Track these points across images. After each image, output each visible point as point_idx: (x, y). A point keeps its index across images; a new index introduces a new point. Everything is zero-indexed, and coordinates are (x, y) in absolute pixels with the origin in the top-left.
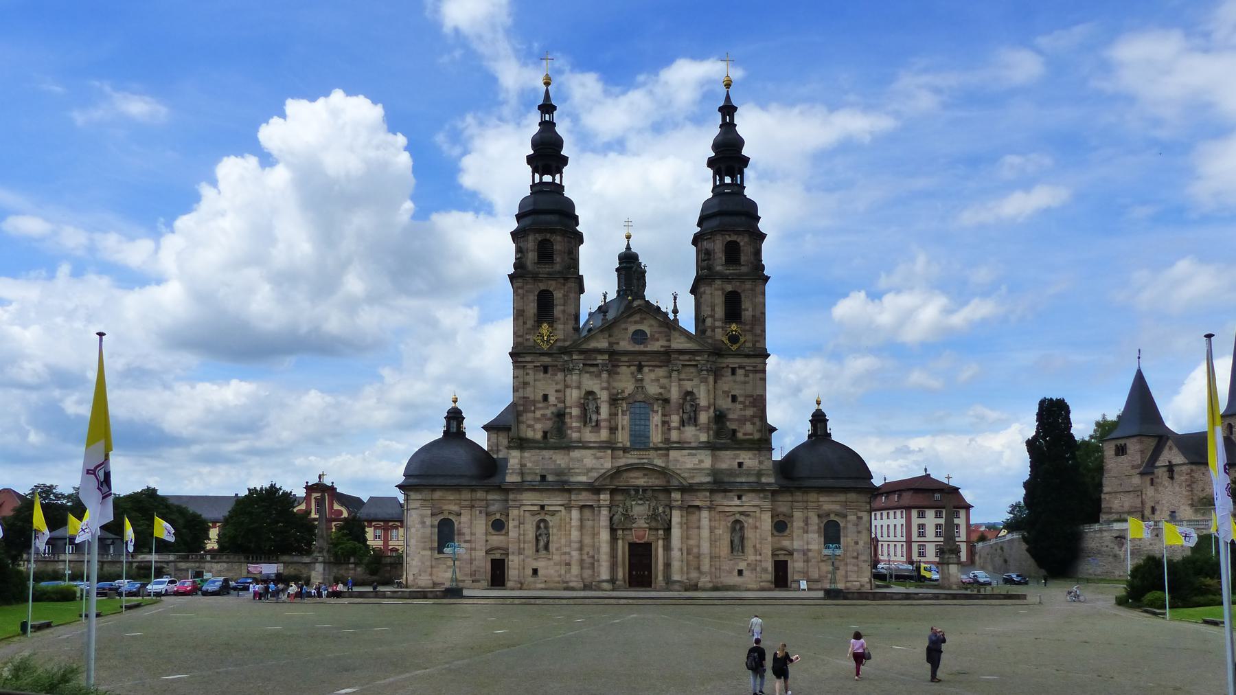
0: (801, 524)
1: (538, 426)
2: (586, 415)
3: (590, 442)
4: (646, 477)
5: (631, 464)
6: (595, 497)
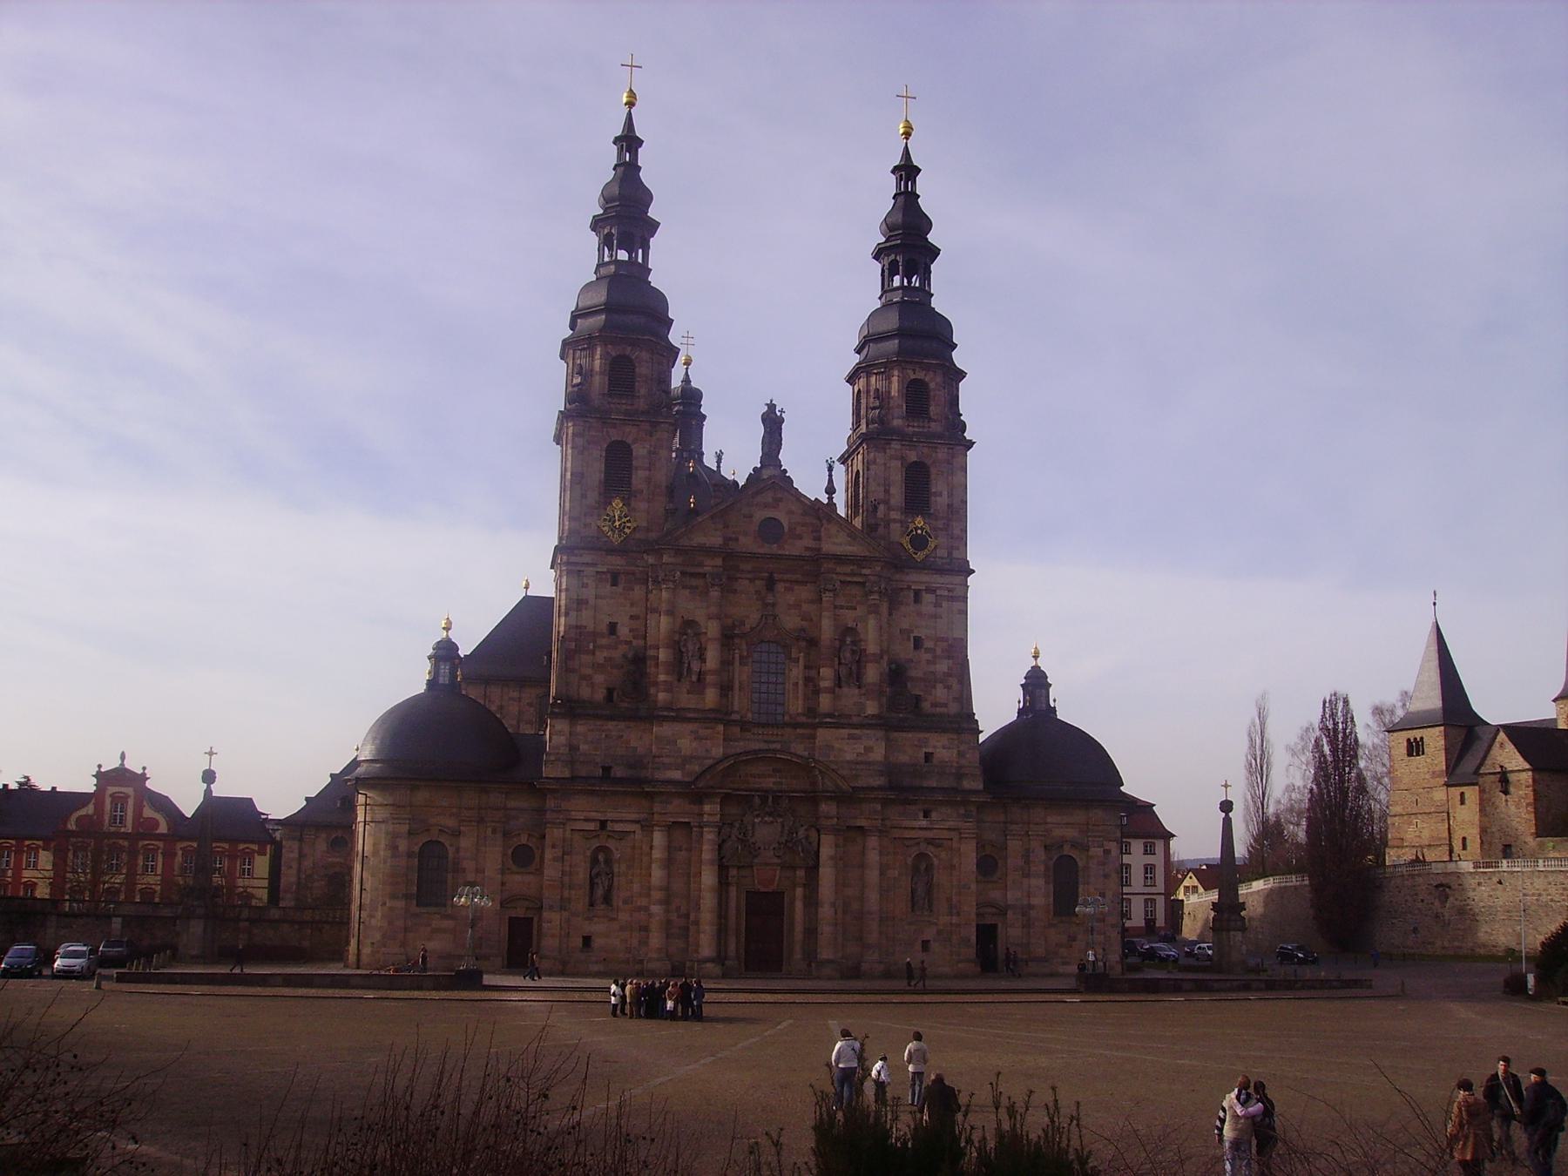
1: (599, 678)
2: (681, 662)
3: (689, 710)
5: (755, 752)
6: (695, 808)
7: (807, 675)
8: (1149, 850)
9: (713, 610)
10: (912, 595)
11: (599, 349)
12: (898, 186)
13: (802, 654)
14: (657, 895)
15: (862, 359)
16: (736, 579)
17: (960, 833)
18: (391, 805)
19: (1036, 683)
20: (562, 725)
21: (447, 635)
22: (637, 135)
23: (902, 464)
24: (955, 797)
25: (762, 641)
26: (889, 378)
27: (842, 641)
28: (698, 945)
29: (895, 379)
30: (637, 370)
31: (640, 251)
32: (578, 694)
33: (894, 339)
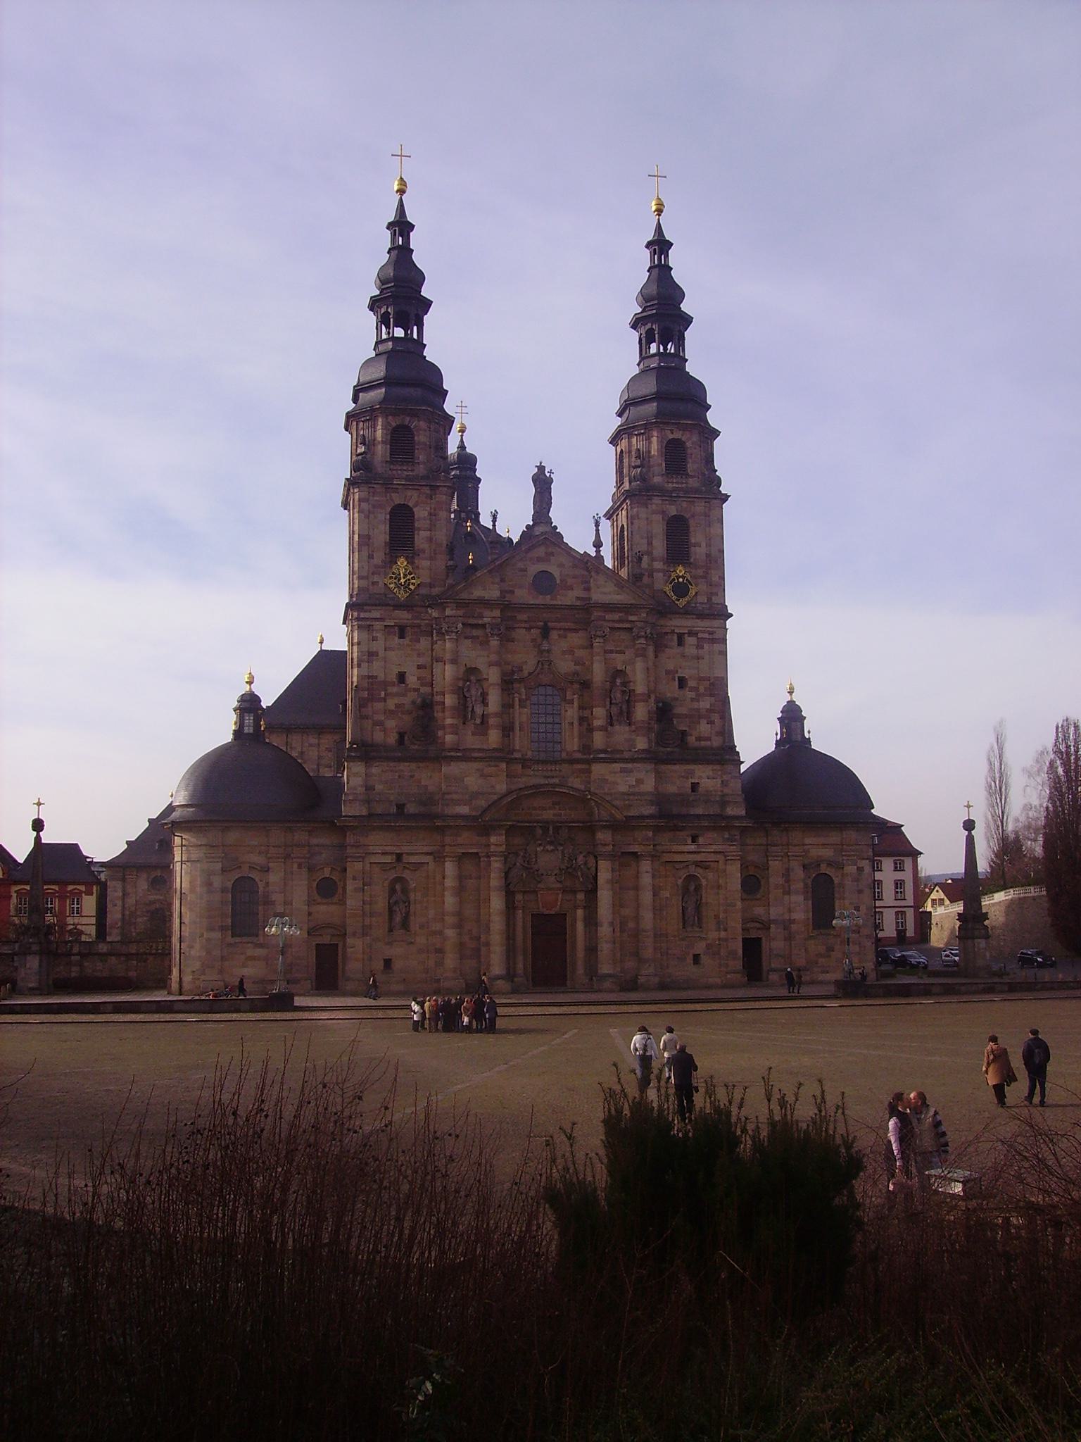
0: (781, 881)
1: (391, 724)
2: (466, 707)
4: (557, 807)
5: (534, 786)
7: (581, 715)
8: (898, 867)
9: (494, 657)
10: (675, 637)
11: (380, 420)
12: (652, 259)
13: (576, 696)
14: (450, 920)
15: (623, 421)
16: (514, 628)
17: (725, 857)
18: (206, 845)
19: (791, 717)
20: (359, 768)
21: (250, 688)
22: (408, 220)
23: (663, 518)
24: (719, 823)
25: (540, 685)
26: (649, 439)
27: (613, 683)
28: (489, 965)
29: (654, 440)
30: (416, 438)
31: (415, 328)
32: (373, 739)
33: (654, 402)
